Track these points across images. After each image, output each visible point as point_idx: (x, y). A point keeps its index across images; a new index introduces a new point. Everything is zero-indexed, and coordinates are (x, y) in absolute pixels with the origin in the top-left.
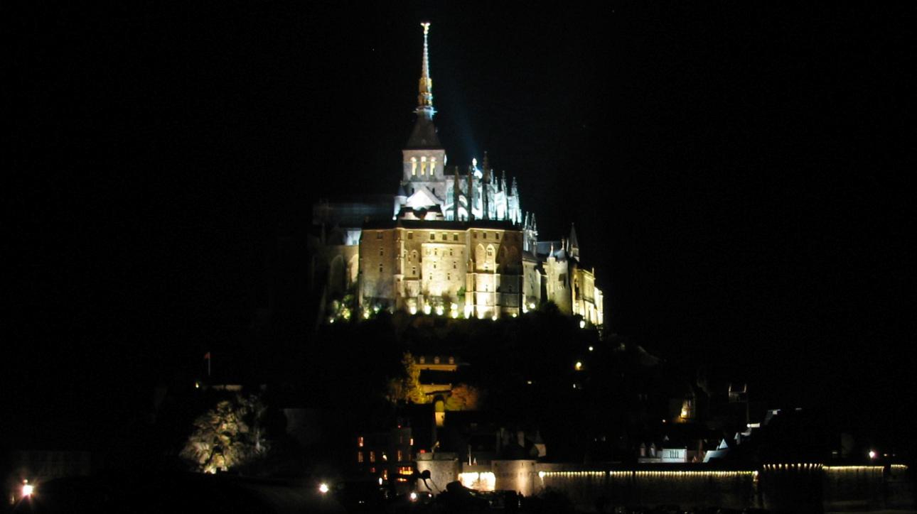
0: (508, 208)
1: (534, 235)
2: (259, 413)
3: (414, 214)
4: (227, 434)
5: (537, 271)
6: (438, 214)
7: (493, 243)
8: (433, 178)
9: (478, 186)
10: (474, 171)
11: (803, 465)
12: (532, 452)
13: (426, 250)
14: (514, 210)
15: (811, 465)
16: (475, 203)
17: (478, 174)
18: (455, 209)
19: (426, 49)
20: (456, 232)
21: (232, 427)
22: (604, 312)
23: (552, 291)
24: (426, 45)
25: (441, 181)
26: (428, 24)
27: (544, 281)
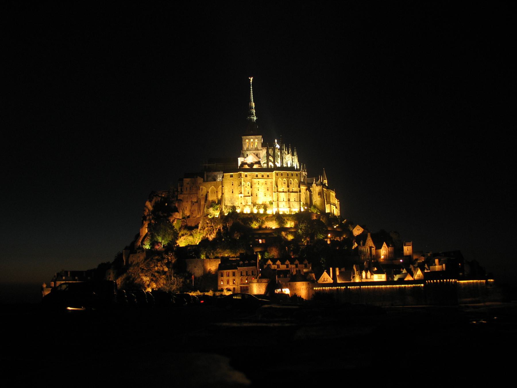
0: (293, 162)
1: (305, 174)
2: (173, 262)
3: (248, 166)
5: (307, 191)
6: (259, 165)
8: (257, 149)
9: (278, 152)
10: (276, 145)
12: (308, 277)
14: (296, 163)
15: (451, 280)
16: (277, 160)
17: (278, 146)
18: (267, 163)
20: (268, 173)
21: (160, 269)
22: (340, 210)
23: (315, 200)
24: (251, 87)
25: (262, 150)
26: (252, 78)
27: (311, 196)
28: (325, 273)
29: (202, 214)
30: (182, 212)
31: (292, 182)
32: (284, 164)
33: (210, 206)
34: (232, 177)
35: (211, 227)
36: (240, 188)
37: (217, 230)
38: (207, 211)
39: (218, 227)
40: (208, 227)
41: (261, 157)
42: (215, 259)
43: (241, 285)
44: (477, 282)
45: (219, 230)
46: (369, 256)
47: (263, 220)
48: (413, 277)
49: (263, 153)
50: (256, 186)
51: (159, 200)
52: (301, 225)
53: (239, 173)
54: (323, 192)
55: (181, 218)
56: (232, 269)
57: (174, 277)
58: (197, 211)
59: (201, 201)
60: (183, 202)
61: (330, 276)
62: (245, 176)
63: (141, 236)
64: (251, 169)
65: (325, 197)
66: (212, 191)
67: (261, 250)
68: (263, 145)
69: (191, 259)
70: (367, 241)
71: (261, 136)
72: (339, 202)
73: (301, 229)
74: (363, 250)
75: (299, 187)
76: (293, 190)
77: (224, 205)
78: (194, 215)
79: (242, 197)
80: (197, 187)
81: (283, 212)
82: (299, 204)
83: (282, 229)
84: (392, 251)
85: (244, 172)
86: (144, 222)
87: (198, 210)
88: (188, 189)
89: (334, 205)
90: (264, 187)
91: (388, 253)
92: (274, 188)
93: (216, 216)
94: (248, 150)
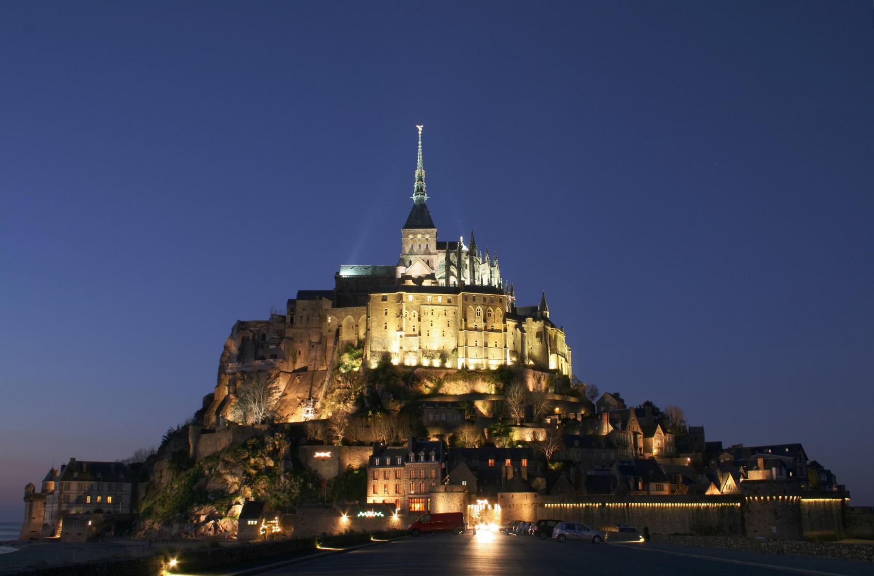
0: (491, 277)
2: (283, 451)
3: (413, 281)
4: (255, 468)
5: (518, 329)
6: (433, 281)
9: (465, 259)
11: (783, 498)
12: (534, 485)
14: (496, 279)
15: (791, 497)
16: (463, 273)
17: (465, 248)
18: (447, 278)
19: (420, 146)
20: (450, 296)
21: (259, 462)
23: (531, 346)
24: (420, 143)
25: (436, 254)
26: (422, 126)
27: (523, 337)
29: (328, 363)
31: (493, 313)
32: (476, 281)
34: (386, 300)
36: (399, 320)
37: (358, 394)
39: (359, 388)
40: (339, 388)
41: (435, 266)
42: (360, 448)
44: (830, 502)
45: (362, 394)
46: (632, 450)
47: (441, 380)
48: (720, 490)
49: (439, 259)
53: (397, 295)
55: (290, 371)
57: (284, 478)
60: (294, 342)
63: (216, 401)
64: (418, 287)
66: (349, 323)
67: (439, 433)
68: (440, 246)
69: (316, 446)
70: (629, 421)
71: (435, 230)
72: (569, 350)
74: (623, 438)
75: (504, 322)
76: (493, 326)
79: (403, 336)
80: (320, 315)
81: (476, 365)
84: (671, 441)
85: (407, 292)
86: (223, 376)
87: (321, 357)
88: (304, 318)
89: (562, 356)
91: (664, 445)
94: (411, 253)
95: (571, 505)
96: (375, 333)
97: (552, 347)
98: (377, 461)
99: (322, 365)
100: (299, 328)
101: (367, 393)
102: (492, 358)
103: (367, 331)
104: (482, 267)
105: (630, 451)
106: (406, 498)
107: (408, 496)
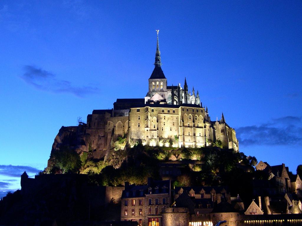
0: (196, 102)
5: (211, 128)
7: (191, 113)
8: (162, 90)
9: (182, 93)
10: (180, 88)
13: (160, 117)
20: (174, 109)
23: (218, 137)
27: (214, 132)
28: (253, 202)
29: (108, 146)
30: (89, 146)
33: (116, 139)
34: (139, 111)
35: (116, 159)
36: (146, 122)
37: (123, 161)
38: (113, 144)
39: (124, 159)
40: (113, 159)
42: (119, 188)
43: (149, 216)
45: (125, 161)
49: (169, 94)
50: (163, 120)
51: (68, 134)
52: (210, 156)
54: (226, 129)
56: (138, 197)
58: (103, 146)
59: (108, 135)
61: (258, 205)
62: (151, 111)
65: (227, 134)
66: (119, 126)
73: (211, 160)
77: (131, 138)
78: (101, 149)
79: (149, 130)
81: (189, 146)
82: (204, 140)
83: (188, 161)
88: (96, 124)
90: (170, 122)
92: (180, 123)
93: (122, 149)
95: (263, 221)
96: (133, 129)
97: (230, 138)
98: (128, 194)
99: (104, 147)
100: (93, 129)
101: (128, 160)
102: (198, 142)
103: (128, 128)
104: (191, 97)
105: (284, 189)
106: (147, 218)
107: (147, 217)
